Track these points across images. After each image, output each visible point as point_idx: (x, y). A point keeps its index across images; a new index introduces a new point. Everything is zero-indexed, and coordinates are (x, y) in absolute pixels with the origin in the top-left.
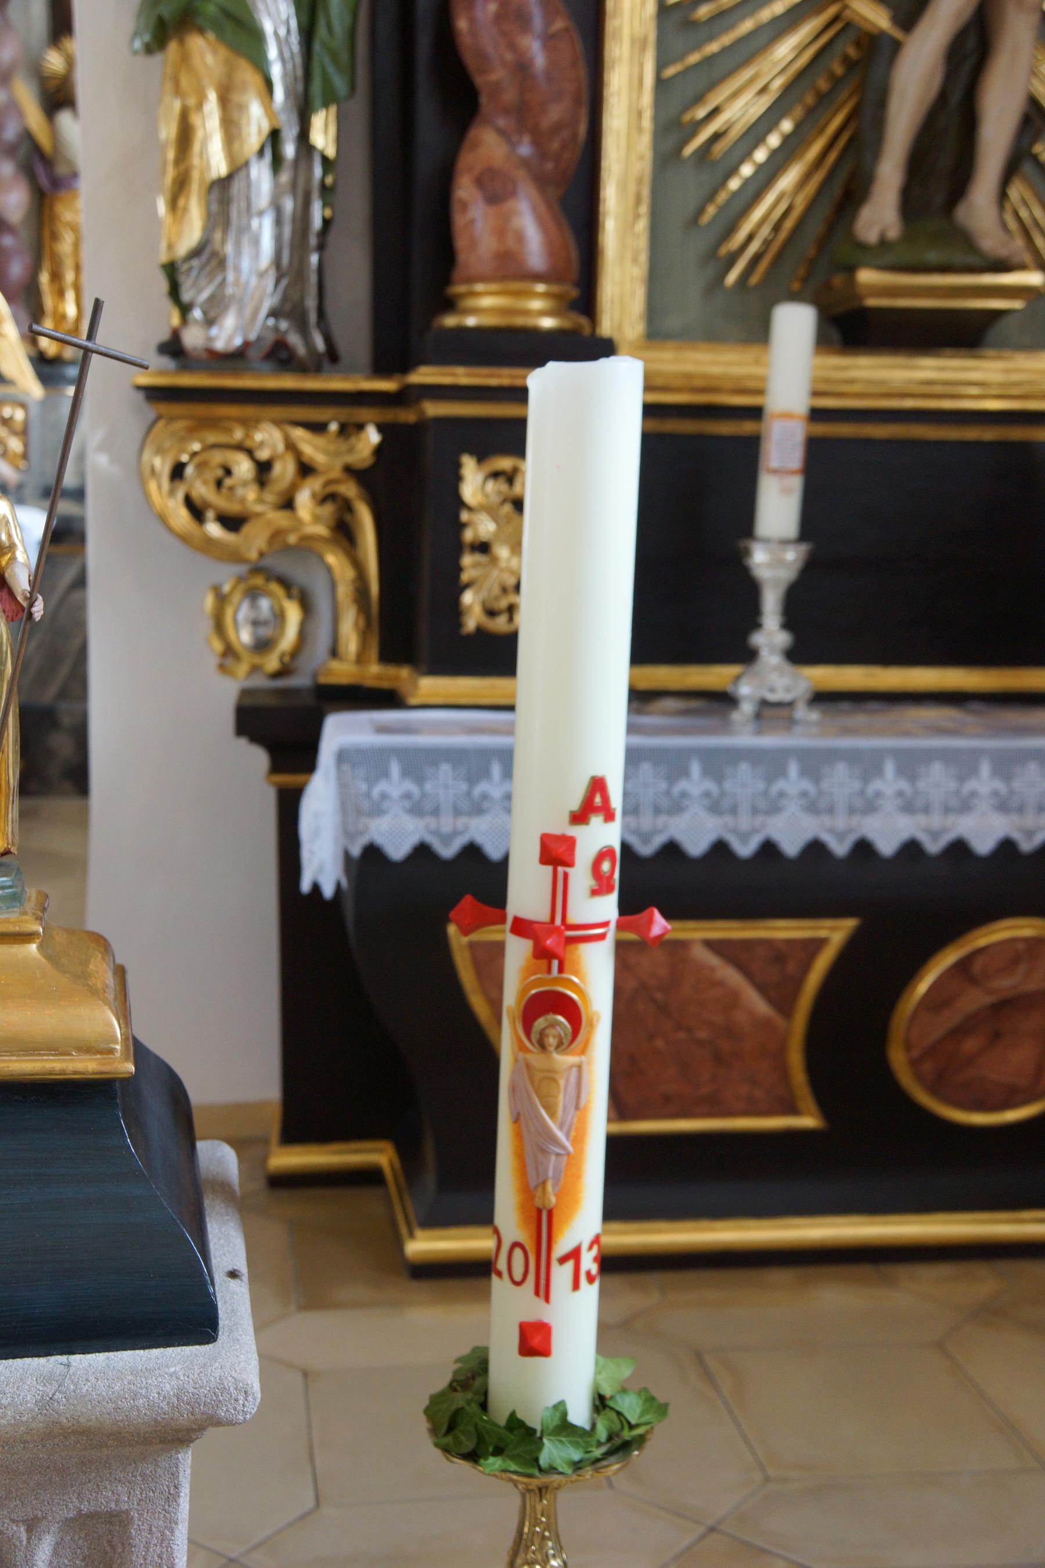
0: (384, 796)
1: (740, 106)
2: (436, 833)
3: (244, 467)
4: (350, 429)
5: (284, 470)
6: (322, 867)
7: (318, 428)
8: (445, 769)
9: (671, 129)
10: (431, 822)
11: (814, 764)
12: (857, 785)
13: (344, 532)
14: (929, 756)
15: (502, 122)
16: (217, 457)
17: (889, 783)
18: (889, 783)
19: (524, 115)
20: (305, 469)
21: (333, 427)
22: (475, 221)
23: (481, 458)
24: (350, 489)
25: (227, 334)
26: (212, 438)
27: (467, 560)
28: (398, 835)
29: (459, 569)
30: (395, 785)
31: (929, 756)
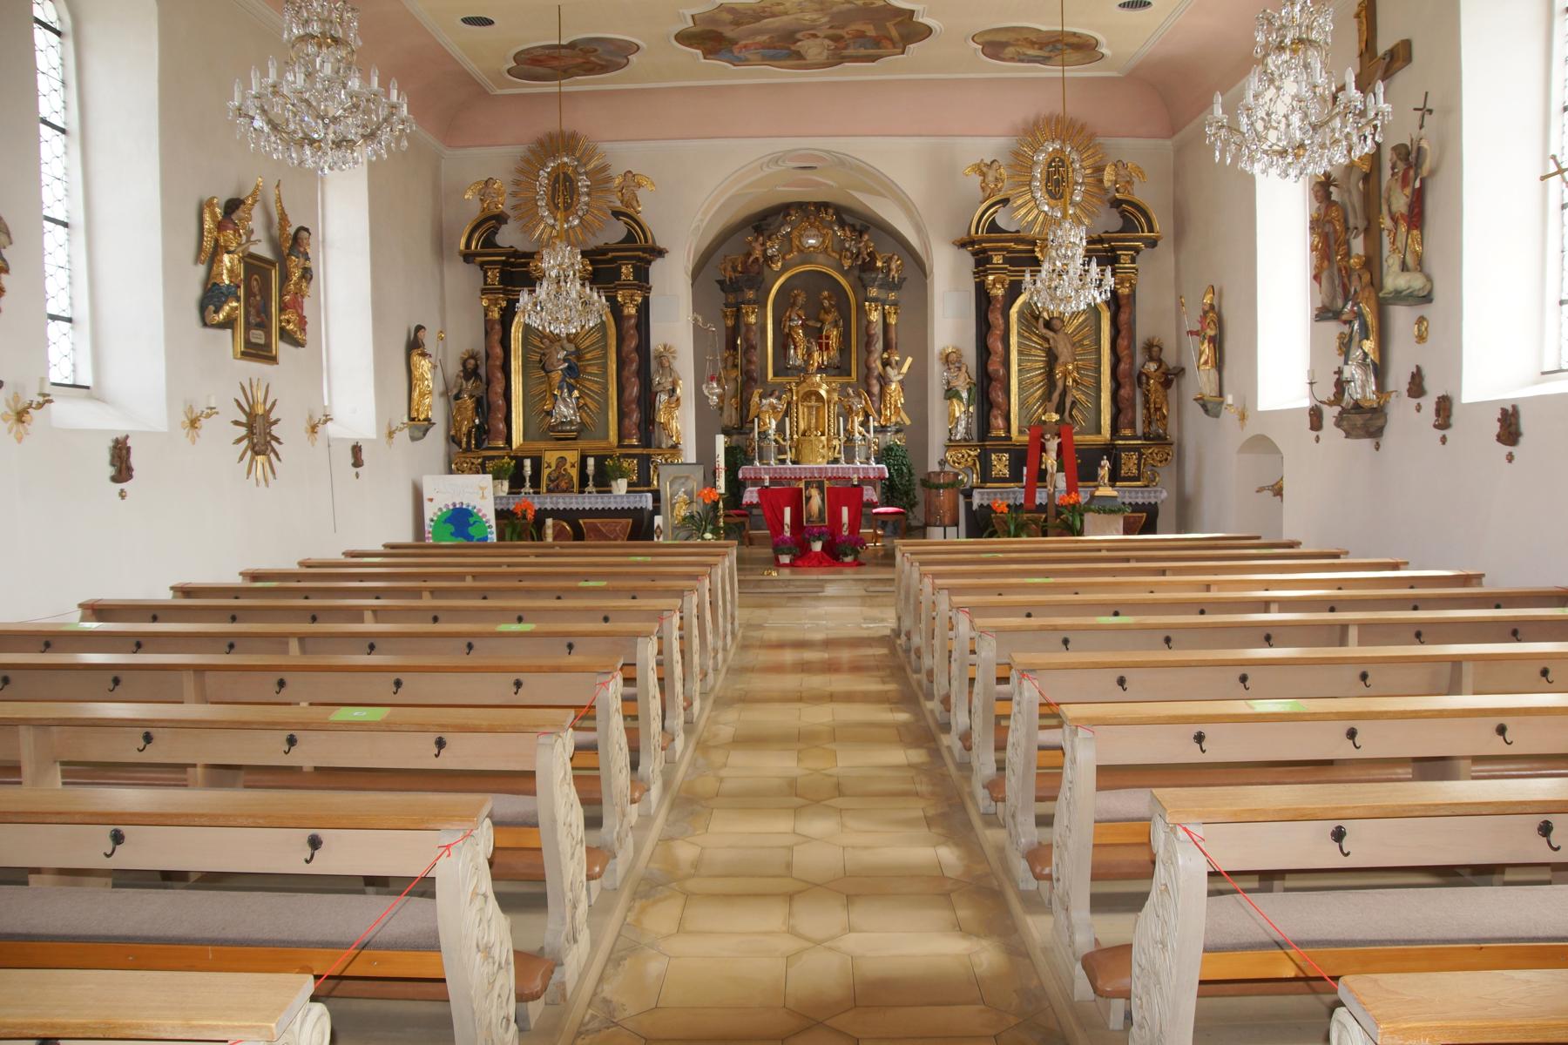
1: (1031, 400)
6: (975, 507)
9: (1022, 404)
22: (993, 421)
28: (985, 503)
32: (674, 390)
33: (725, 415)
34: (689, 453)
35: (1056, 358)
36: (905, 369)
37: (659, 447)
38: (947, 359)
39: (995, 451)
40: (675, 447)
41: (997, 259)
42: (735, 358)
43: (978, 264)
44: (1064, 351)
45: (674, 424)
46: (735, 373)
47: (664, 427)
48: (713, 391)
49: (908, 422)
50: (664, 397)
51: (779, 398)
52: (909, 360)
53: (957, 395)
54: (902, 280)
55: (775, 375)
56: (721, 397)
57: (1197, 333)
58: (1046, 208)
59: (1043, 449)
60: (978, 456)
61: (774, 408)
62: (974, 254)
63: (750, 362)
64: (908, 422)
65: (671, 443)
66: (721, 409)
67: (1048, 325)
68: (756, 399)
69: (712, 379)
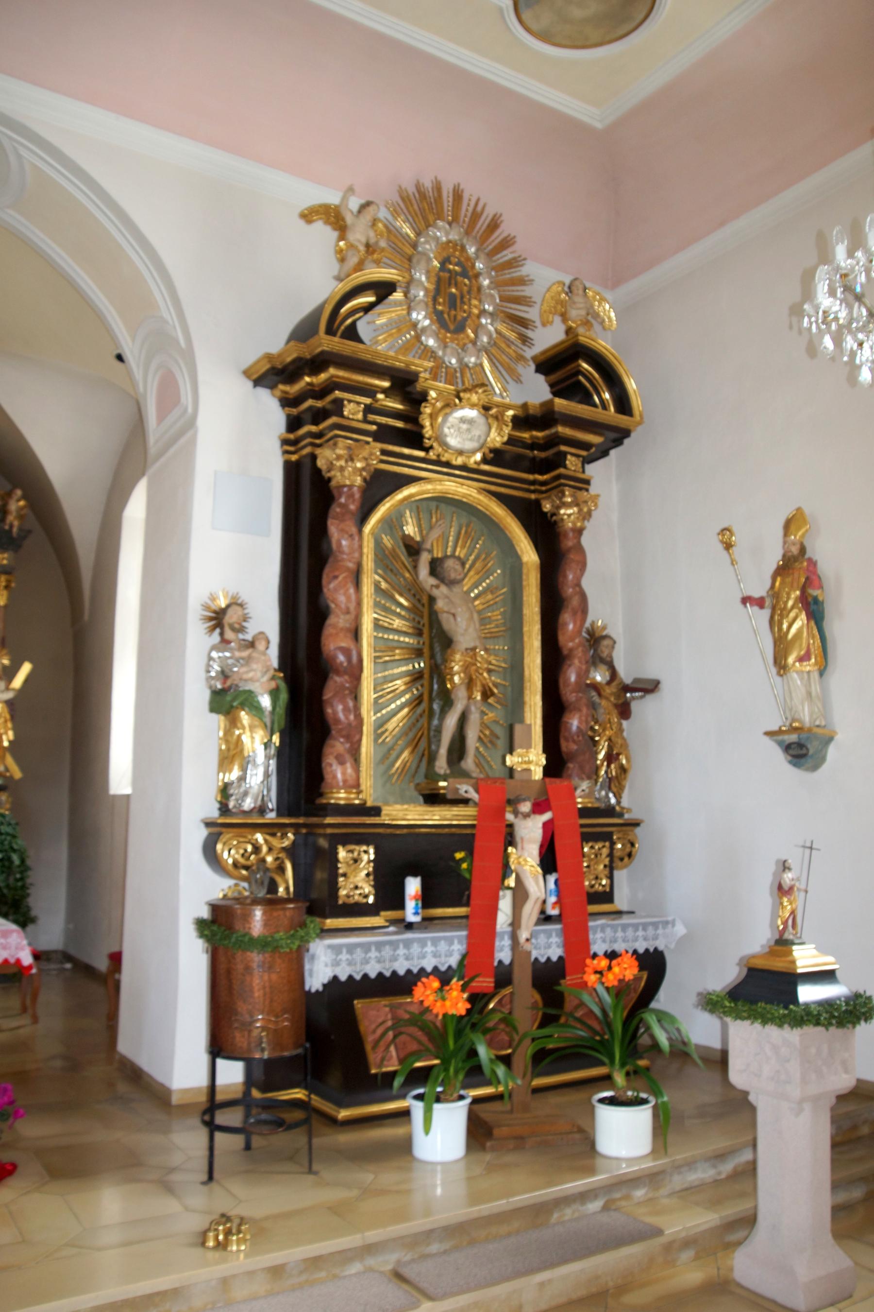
0: (341, 960)
2: (355, 972)
3: (250, 848)
4: (284, 836)
5: (265, 849)
7: (273, 835)
8: (359, 950)
10: (382, 965)
11: (379, 946)
12: (420, 950)
13: (281, 869)
14: (440, 939)
15: (342, 740)
16: (243, 845)
17: (429, 948)
18: (429, 948)
19: (348, 737)
20: (270, 850)
21: (279, 834)
23: (344, 845)
24: (282, 855)
25: (248, 804)
26: (242, 840)
27: (341, 879)
29: (337, 883)
30: (344, 956)
31: (440, 939)
35: (447, 642)
36: (18, 682)
38: (217, 619)
39: (348, 839)
41: (353, 409)
43: (293, 424)
44: (464, 630)
49: (17, 774)
52: (26, 668)
53: (249, 701)
54: (25, 533)
57: (760, 603)
58: (431, 342)
59: (510, 839)
60: (291, 852)
62: (286, 402)
64: (17, 774)
67: (435, 568)
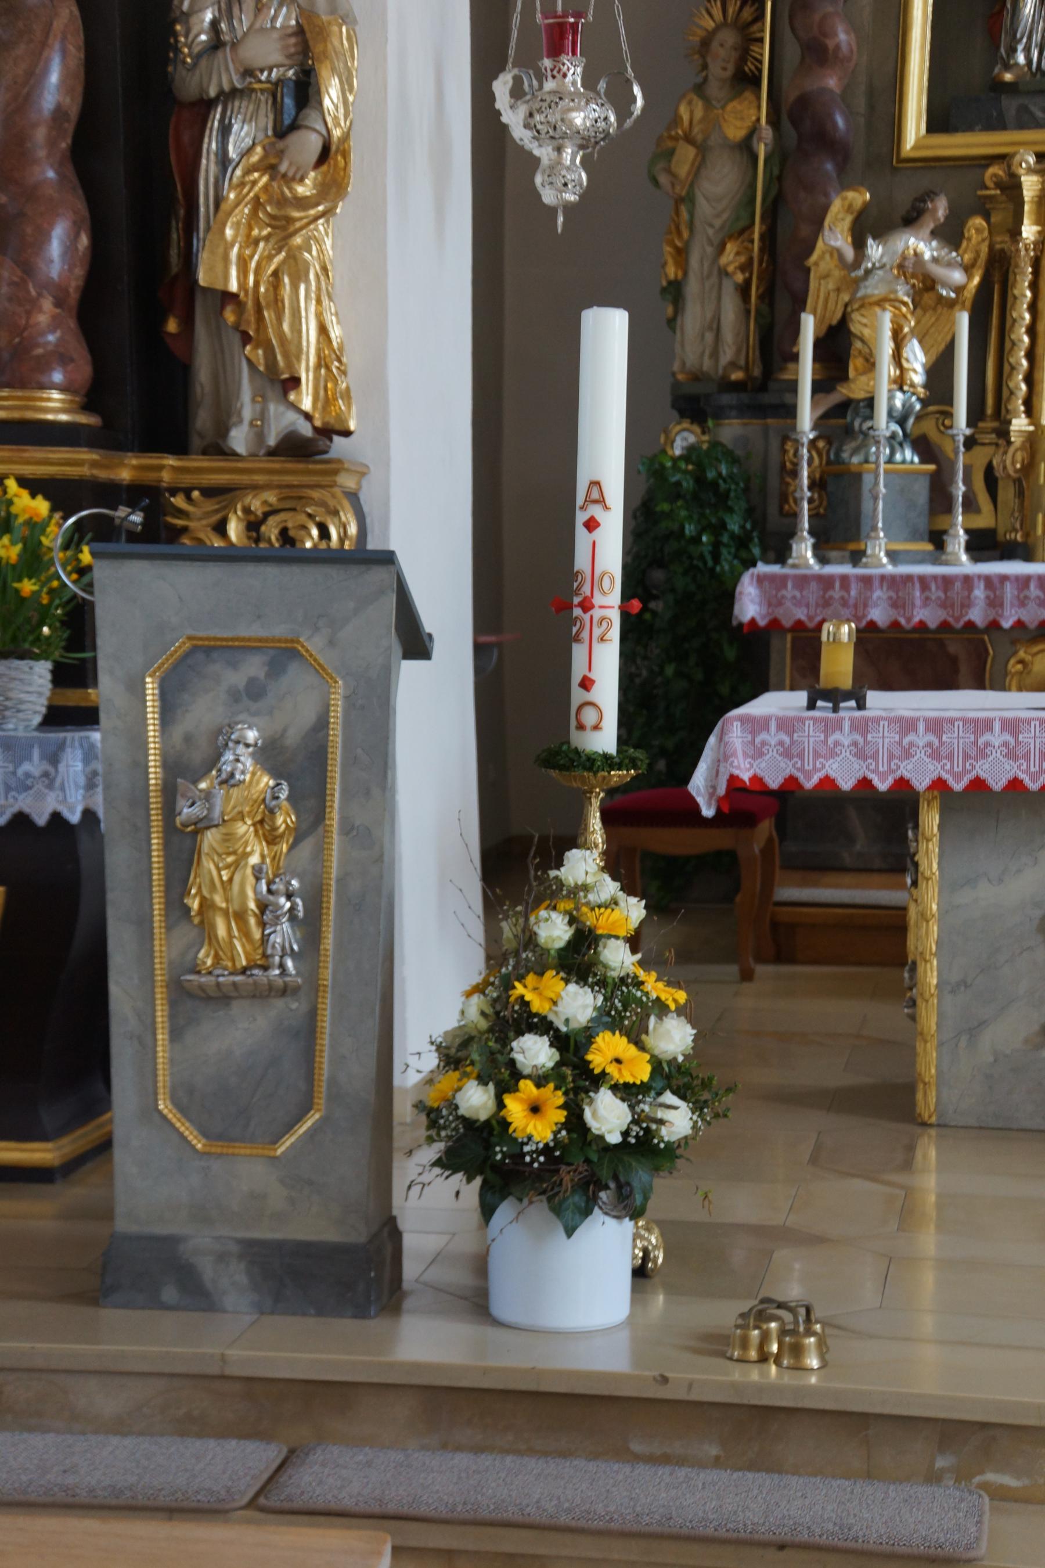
32: (305, 91)
33: (693, 318)
34: (421, 504)
37: (218, 449)
40: (308, 450)
42: (749, 40)
45: (309, 320)
46: (747, 116)
47: (249, 320)
48: (570, 118)
50: (244, 134)
51: (950, 235)
55: (939, 121)
56: (598, 152)
61: (925, 285)
63: (818, 53)
65: (282, 421)
66: (675, 292)
68: (836, 237)
69: (558, 39)
